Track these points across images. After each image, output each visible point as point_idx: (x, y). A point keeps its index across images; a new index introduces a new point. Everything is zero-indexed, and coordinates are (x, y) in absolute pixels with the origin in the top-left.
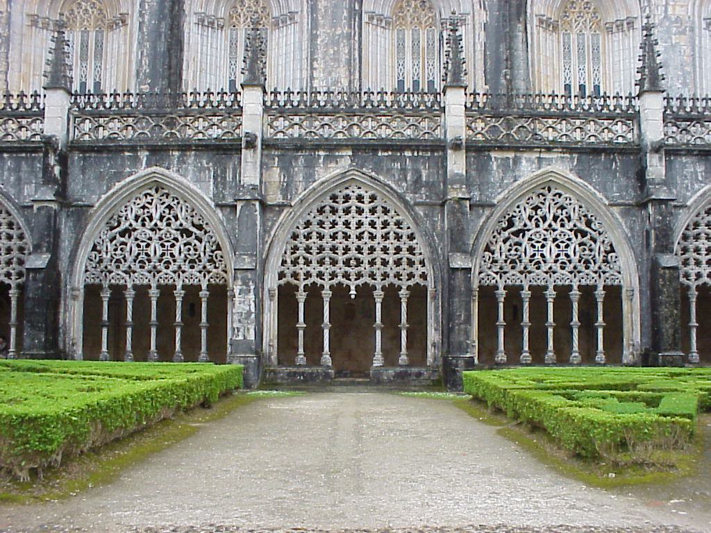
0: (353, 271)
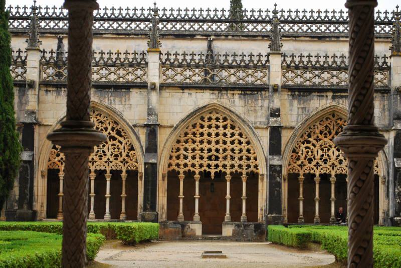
0: (213, 163)
